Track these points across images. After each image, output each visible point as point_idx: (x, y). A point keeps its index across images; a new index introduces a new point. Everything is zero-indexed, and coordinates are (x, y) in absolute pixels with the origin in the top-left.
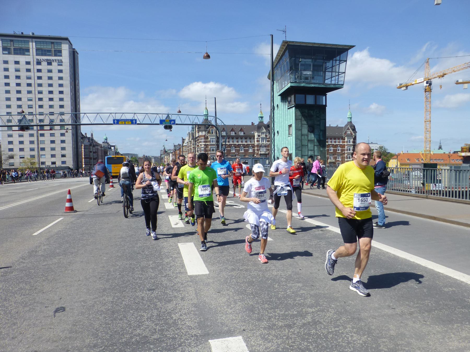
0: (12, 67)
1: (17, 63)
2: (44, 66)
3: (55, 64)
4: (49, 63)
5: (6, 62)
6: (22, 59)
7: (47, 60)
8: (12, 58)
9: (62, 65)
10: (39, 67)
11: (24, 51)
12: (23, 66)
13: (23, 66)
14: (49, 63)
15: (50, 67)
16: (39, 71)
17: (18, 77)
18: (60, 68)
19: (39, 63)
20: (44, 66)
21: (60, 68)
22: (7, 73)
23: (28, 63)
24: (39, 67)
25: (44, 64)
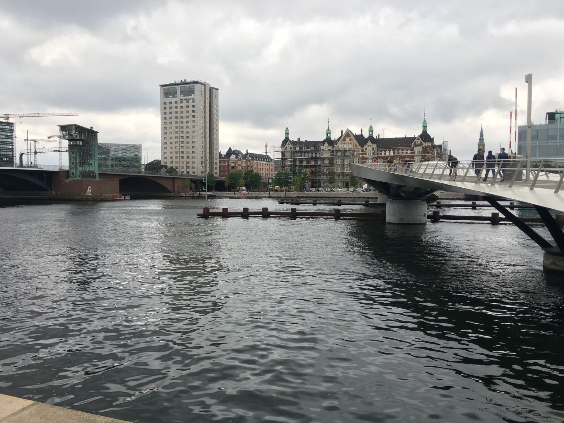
0: (168, 106)
1: (171, 103)
2: (184, 104)
3: (190, 101)
4: (188, 102)
5: (165, 103)
6: (173, 100)
7: (186, 99)
8: (167, 100)
9: (194, 102)
10: (182, 105)
11: (174, 94)
12: (173, 105)
13: (173, 105)
14: (188, 102)
15: (187, 104)
16: (182, 107)
17: (171, 113)
18: (193, 104)
19: (182, 102)
20: (184, 104)
21: (193, 104)
22: (165, 111)
23: (176, 102)
24: (182, 105)
25: (185, 102)
